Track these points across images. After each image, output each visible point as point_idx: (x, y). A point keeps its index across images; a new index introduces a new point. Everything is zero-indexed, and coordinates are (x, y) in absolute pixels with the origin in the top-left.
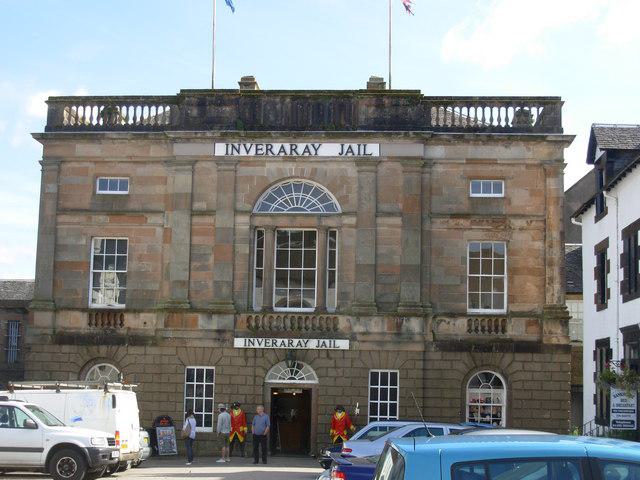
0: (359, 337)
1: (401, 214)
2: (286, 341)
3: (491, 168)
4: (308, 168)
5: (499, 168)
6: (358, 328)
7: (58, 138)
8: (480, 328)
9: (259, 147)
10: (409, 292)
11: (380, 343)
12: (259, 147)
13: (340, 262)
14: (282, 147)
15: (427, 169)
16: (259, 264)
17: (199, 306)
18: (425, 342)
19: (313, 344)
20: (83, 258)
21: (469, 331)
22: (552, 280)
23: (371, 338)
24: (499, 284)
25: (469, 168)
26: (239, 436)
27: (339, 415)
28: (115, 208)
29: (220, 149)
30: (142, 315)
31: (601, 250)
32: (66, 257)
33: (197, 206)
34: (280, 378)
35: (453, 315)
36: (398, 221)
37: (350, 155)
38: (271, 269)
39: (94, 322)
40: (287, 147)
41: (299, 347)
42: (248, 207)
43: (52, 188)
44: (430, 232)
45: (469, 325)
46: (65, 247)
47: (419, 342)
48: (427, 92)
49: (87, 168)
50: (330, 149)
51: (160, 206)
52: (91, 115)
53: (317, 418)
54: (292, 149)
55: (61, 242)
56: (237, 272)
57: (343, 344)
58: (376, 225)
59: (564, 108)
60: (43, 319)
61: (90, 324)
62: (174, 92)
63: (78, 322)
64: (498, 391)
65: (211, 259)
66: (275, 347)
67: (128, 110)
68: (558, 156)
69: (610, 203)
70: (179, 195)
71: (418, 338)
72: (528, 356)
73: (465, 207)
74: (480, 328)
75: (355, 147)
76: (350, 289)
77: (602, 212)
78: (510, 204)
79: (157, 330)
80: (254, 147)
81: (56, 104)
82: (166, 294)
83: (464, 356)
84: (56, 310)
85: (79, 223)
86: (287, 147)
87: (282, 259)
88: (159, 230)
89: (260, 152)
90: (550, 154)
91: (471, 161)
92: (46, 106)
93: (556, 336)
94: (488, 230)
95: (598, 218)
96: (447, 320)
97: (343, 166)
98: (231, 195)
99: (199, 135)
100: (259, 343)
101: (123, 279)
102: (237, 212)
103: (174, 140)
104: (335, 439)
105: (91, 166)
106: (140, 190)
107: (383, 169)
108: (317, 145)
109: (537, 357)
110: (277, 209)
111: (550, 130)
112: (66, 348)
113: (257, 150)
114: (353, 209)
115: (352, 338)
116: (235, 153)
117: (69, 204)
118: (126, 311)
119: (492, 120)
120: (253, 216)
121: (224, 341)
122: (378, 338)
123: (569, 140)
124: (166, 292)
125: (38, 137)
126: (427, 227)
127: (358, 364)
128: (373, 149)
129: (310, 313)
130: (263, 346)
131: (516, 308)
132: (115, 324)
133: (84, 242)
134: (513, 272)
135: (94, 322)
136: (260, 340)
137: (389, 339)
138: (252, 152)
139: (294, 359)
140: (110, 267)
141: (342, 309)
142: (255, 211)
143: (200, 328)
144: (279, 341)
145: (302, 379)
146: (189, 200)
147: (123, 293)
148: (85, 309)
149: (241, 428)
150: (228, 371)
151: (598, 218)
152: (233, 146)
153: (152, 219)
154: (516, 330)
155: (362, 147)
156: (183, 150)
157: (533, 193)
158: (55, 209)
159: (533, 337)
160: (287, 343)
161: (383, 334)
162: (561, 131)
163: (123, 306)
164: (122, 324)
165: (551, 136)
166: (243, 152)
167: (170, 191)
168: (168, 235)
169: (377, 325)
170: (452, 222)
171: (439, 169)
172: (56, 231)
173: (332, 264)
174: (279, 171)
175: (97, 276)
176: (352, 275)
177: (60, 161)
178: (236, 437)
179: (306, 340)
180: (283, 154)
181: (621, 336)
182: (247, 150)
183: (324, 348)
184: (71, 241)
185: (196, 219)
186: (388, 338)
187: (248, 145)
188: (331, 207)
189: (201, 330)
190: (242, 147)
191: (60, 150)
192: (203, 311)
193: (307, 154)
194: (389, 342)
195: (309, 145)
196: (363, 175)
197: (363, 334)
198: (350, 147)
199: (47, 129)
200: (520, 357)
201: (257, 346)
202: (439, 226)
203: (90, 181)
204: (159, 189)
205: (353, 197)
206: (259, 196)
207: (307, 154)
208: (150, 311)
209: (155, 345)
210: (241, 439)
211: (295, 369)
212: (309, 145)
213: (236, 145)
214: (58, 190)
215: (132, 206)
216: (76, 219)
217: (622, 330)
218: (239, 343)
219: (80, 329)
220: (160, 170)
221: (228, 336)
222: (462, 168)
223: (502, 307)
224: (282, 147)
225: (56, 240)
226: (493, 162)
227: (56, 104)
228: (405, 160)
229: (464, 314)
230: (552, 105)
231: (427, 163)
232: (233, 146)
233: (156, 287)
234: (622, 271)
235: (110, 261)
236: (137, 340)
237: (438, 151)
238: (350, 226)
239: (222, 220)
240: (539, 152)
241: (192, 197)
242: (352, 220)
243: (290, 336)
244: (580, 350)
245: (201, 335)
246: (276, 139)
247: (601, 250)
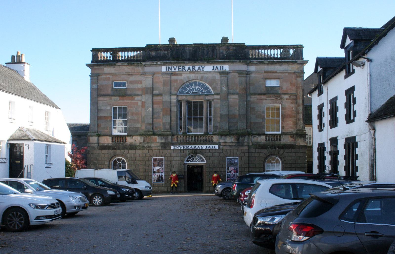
0: (222, 144)
1: (238, 94)
2: (193, 146)
3: (274, 74)
4: (200, 76)
5: (278, 74)
6: (221, 141)
7: (98, 65)
8: (270, 139)
9: (180, 68)
10: (242, 125)
12: (180, 68)
13: (215, 113)
14: (189, 68)
15: (248, 76)
16: (181, 115)
17: (157, 133)
18: (249, 146)
19: (204, 147)
20: (109, 115)
21: (266, 140)
22: (299, 119)
23: (227, 144)
24: (278, 122)
25: (265, 75)
26: (175, 184)
27: (215, 175)
28: (122, 94)
29: (164, 69)
30: (134, 137)
31: (321, 108)
32: (101, 114)
33: (156, 92)
34: (191, 161)
35: (259, 135)
36: (236, 97)
37: (217, 70)
38: (185, 117)
39: (114, 140)
40: (191, 67)
42: (175, 92)
43: (95, 86)
44: (250, 101)
45: (266, 139)
46: (102, 110)
47: (246, 146)
48: (247, 44)
49: (109, 78)
50: (208, 68)
51: (139, 93)
52: (108, 56)
53: (205, 176)
54: (193, 69)
55: (99, 108)
56: (173, 119)
58: (228, 99)
59: (304, 50)
60: (94, 140)
61: (113, 141)
62: (144, 45)
63: (107, 141)
64: (278, 164)
65: (162, 113)
67: (125, 53)
68: (301, 69)
69: (324, 88)
70: (147, 88)
71: (246, 144)
72: (290, 150)
73: (263, 91)
74: (270, 139)
75: (219, 67)
76: (218, 125)
77: (321, 93)
78: (282, 89)
79: (140, 143)
80: (177, 68)
81: (95, 52)
82: (143, 128)
83: (265, 151)
84: (99, 136)
85: (106, 100)
86: (191, 67)
87: (190, 113)
88: (140, 103)
89: (180, 70)
90: (298, 68)
91: (266, 72)
92: (91, 53)
93: (301, 142)
94: (273, 100)
95: (319, 95)
96: (257, 136)
97: (214, 75)
98: (169, 87)
99: (155, 63)
100: (181, 147)
101: (125, 122)
102: (171, 94)
103: (145, 65)
104: (213, 185)
105: (111, 77)
106: (131, 86)
107: (230, 75)
108: (203, 66)
109: (293, 150)
110: (187, 93)
111: (298, 59)
112: (103, 151)
113: (179, 69)
114: (218, 92)
115: (219, 144)
116: (170, 70)
117: (103, 93)
118: (128, 136)
119: (274, 55)
120: (178, 96)
122: (230, 144)
123: (306, 62)
124: (144, 128)
125: (88, 65)
126: (249, 99)
127: (222, 154)
128: (226, 68)
129: (201, 135)
131: (284, 131)
132: (123, 141)
133: (109, 108)
134: (283, 117)
135: (114, 140)
138: (177, 70)
139: (195, 153)
140: (120, 118)
141: (215, 133)
142: (178, 94)
145: (200, 161)
146: (152, 90)
147: (125, 128)
148: (110, 135)
149: (176, 181)
151: (319, 95)
152: (169, 68)
153: (136, 98)
154: (286, 140)
155: (222, 67)
156: (148, 69)
157: (292, 84)
158: (97, 94)
159: (293, 143)
160: (193, 147)
161: (232, 142)
162: (303, 59)
163: (126, 134)
164: (126, 141)
165: (299, 61)
166: (173, 70)
167: (144, 86)
168: (143, 104)
169: (230, 140)
170: (259, 97)
171: (253, 75)
172: (97, 103)
173: (210, 115)
174: (188, 77)
175: (115, 122)
176: (219, 119)
177: (98, 75)
178: (174, 185)
180: (189, 70)
181: (329, 142)
182: (175, 69)
184: (103, 108)
185: (155, 98)
186: (233, 144)
187: (175, 67)
188: (209, 92)
190: (173, 68)
191: (98, 70)
192: (159, 135)
193: (199, 70)
195: (200, 66)
196: (222, 78)
198: (217, 67)
199: (92, 62)
200: (287, 150)
202: (253, 98)
203: (110, 83)
204: (139, 86)
205: (218, 87)
206: (180, 88)
207: (199, 70)
208: (137, 135)
209: (140, 149)
210: (176, 186)
212: (200, 66)
213: (170, 67)
214: (98, 87)
215: (129, 93)
216: (106, 98)
217: (330, 139)
219: (109, 143)
220: (139, 78)
222: (262, 75)
223: (279, 131)
224: (189, 68)
225: (97, 108)
226: (275, 72)
227: (95, 52)
228: (240, 73)
229: (264, 134)
230: (298, 49)
231: (248, 73)
232: (169, 68)
233: (139, 125)
234: (329, 116)
235: (120, 115)
236: (133, 147)
237: (252, 68)
238: (217, 99)
239: (166, 98)
240: (294, 67)
241: (153, 89)
242: (218, 97)
243: (195, 144)
244: (311, 147)
246: (186, 64)
247: (321, 108)
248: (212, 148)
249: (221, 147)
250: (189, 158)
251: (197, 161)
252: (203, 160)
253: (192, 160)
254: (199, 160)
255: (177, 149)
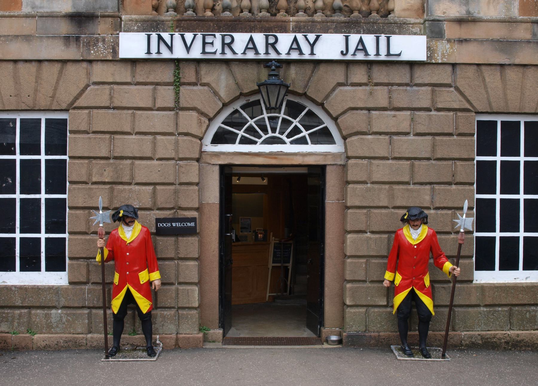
2: (259, 38)
11: (505, 45)
34: (244, 141)
41: (295, 56)
53: (348, 243)
57: (411, 47)
66: (229, 55)
100: (184, 46)
104: (399, 299)
121: (92, 43)
122: (498, 32)
127: (449, 98)
130: (196, 53)
136: (189, 36)
137: (528, 36)
143: (26, 9)
144: (241, 39)
145: (302, 141)
150: (104, 120)
161: (511, 22)
179: (312, 37)
183: (360, 56)
186: (522, 33)
189: (27, 16)
194: (528, 42)
197: (460, 21)
201: (179, 52)
211: (296, 122)
218: (133, 45)
221: (102, 28)
245: (28, 27)
248: (378, 54)
249: (445, 51)
250: (235, 121)
251: (284, 143)
252: (324, 136)
253: (250, 130)
254: (296, 131)
255: (166, 54)
